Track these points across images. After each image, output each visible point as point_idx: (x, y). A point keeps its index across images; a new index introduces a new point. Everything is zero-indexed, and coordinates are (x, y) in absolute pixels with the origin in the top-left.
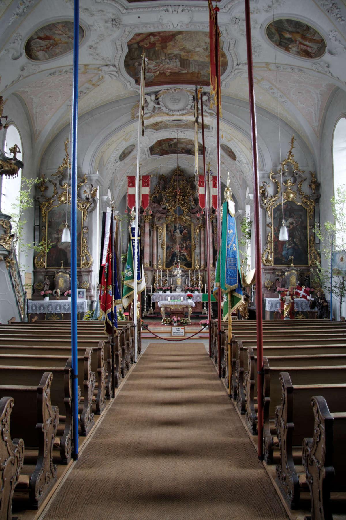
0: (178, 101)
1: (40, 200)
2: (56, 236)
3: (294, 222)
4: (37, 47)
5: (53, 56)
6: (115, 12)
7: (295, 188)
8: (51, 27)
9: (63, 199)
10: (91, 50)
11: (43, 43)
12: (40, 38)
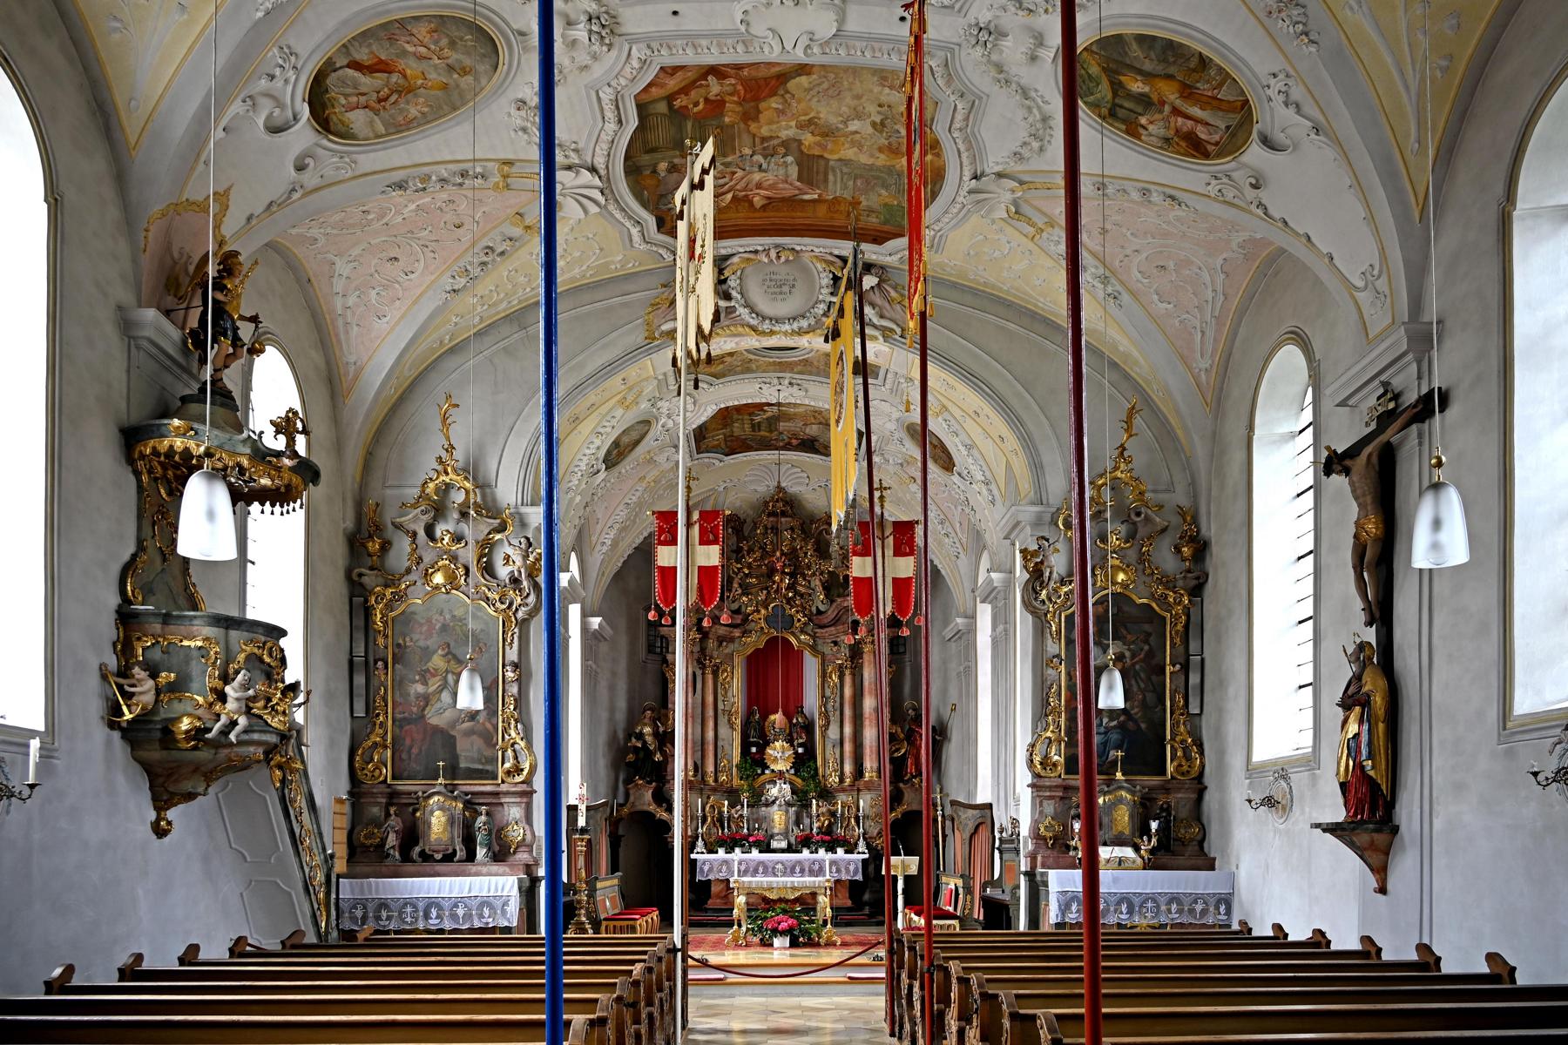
0: (786, 289)
2: (420, 688)
3: (1127, 654)
7: (1132, 555)
9: (439, 578)
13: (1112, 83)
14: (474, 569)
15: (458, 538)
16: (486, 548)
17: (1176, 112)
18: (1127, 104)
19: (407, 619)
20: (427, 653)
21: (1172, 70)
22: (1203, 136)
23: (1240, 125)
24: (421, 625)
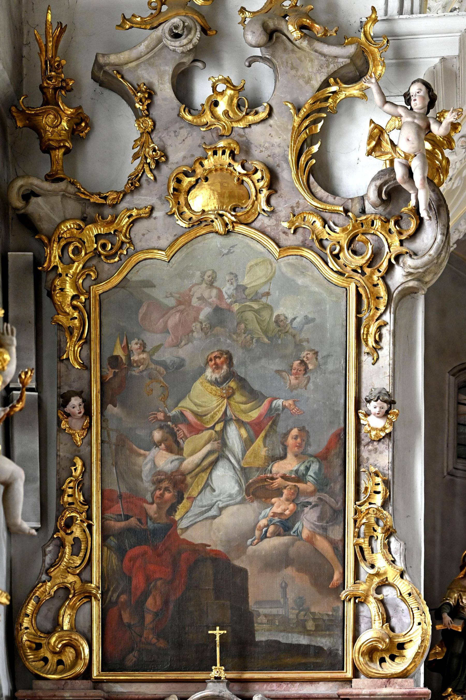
1: (38, 207)
2: (164, 461)
9: (202, 199)
14: (288, 175)
15: (247, 103)
16: (317, 122)
19: (132, 296)
20: (179, 378)
24: (166, 311)
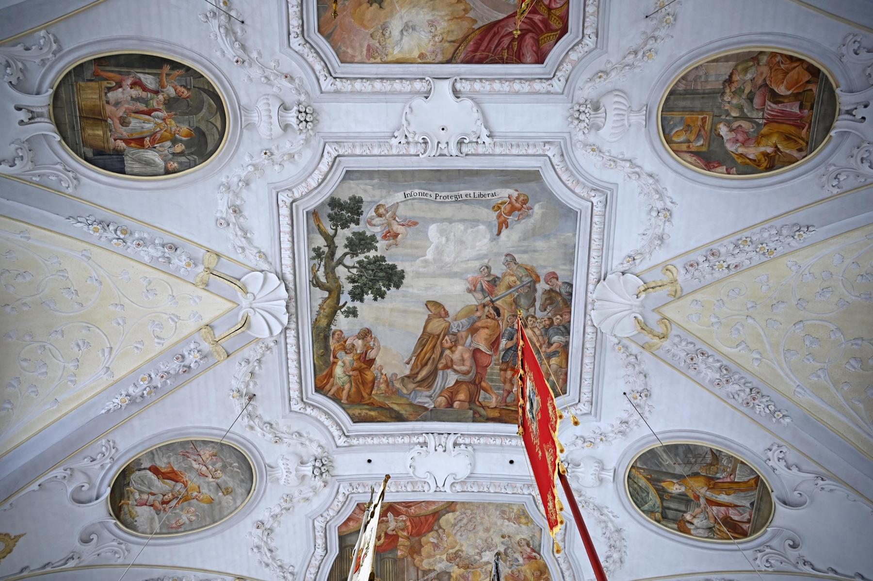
4: (141, 492)
5: (172, 529)
6: (323, 442)
8: (188, 448)
10: (259, 531)
11: (160, 485)
12: (155, 470)
13: (657, 490)
17: (710, 502)
18: (672, 506)
21: (696, 469)
22: (736, 518)
23: (760, 499)
